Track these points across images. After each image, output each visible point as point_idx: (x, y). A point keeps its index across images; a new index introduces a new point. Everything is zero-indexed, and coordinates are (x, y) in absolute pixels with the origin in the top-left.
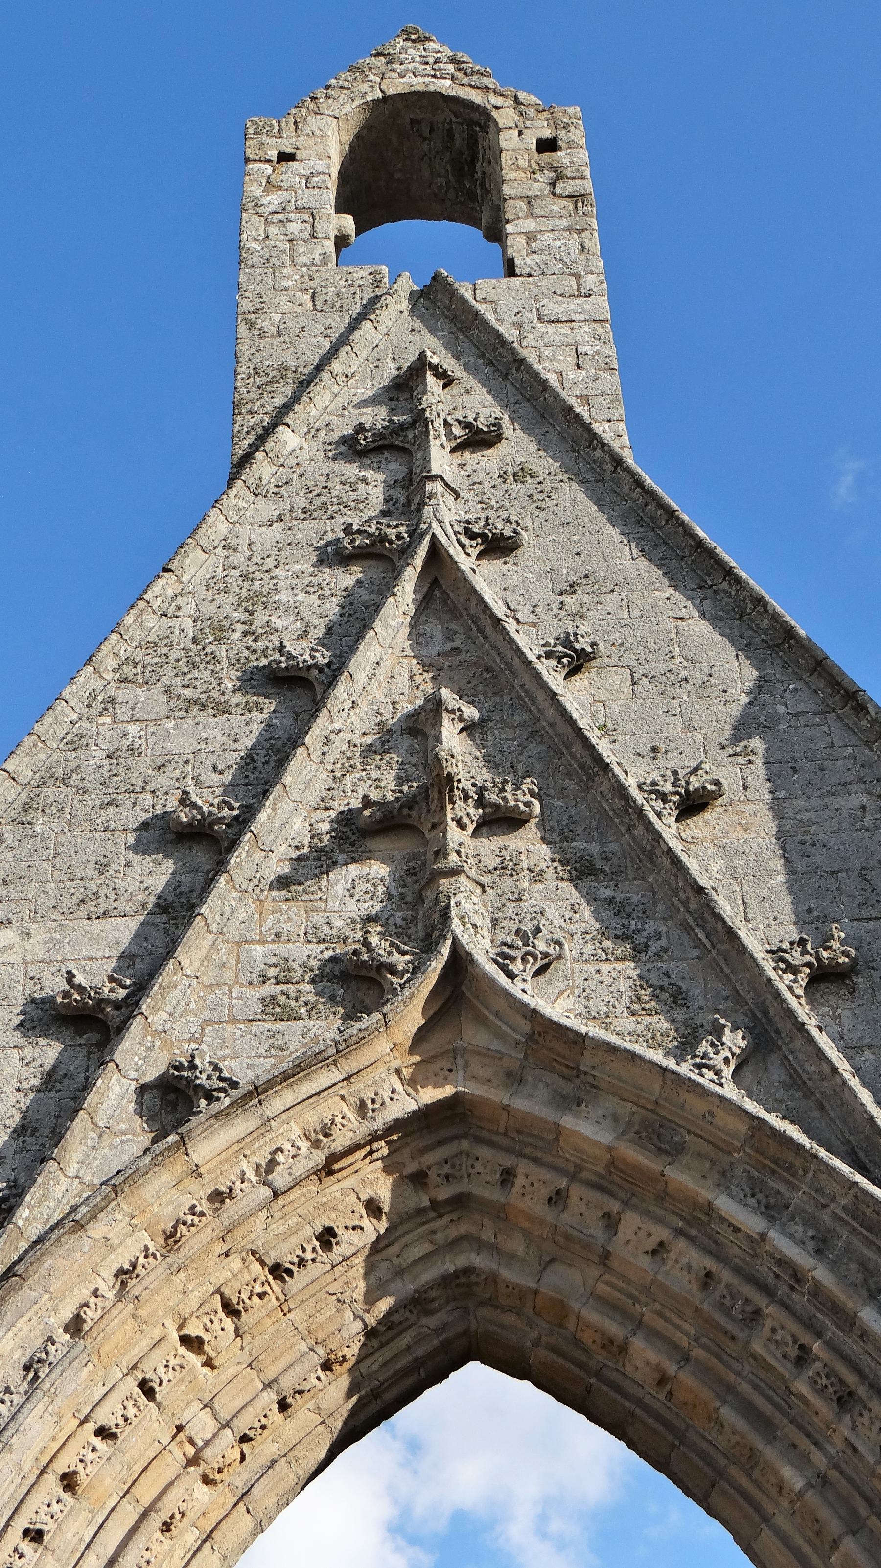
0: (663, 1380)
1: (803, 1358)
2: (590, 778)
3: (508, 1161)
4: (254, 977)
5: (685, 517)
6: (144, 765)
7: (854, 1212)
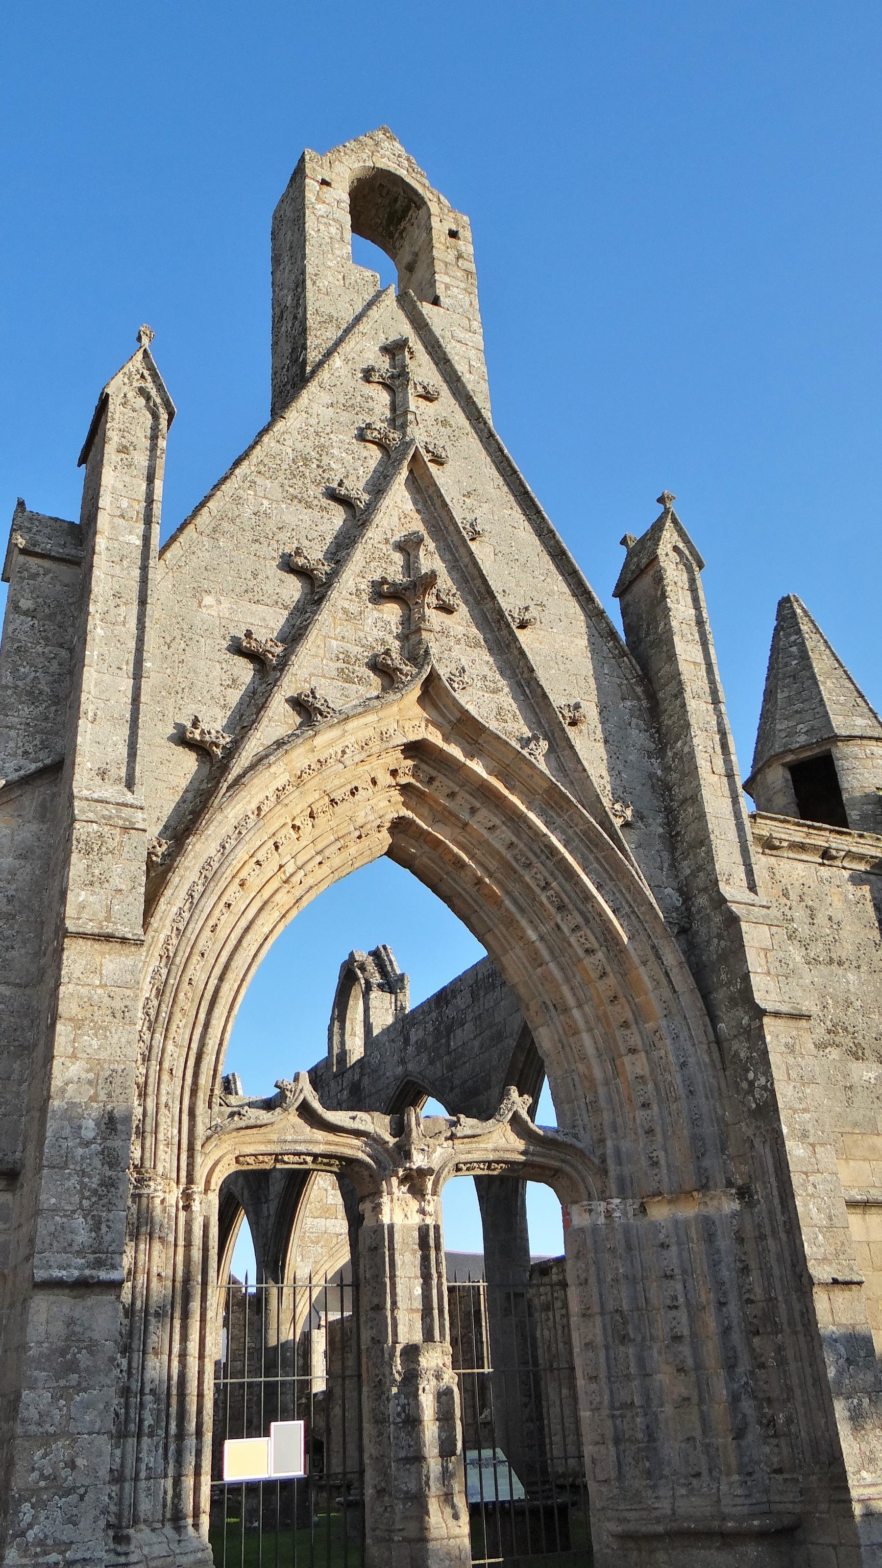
0: (479, 882)
1: (546, 887)
2: (483, 599)
3: (434, 773)
4: (333, 656)
5: (521, 476)
6: (272, 525)
7: (585, 833)
